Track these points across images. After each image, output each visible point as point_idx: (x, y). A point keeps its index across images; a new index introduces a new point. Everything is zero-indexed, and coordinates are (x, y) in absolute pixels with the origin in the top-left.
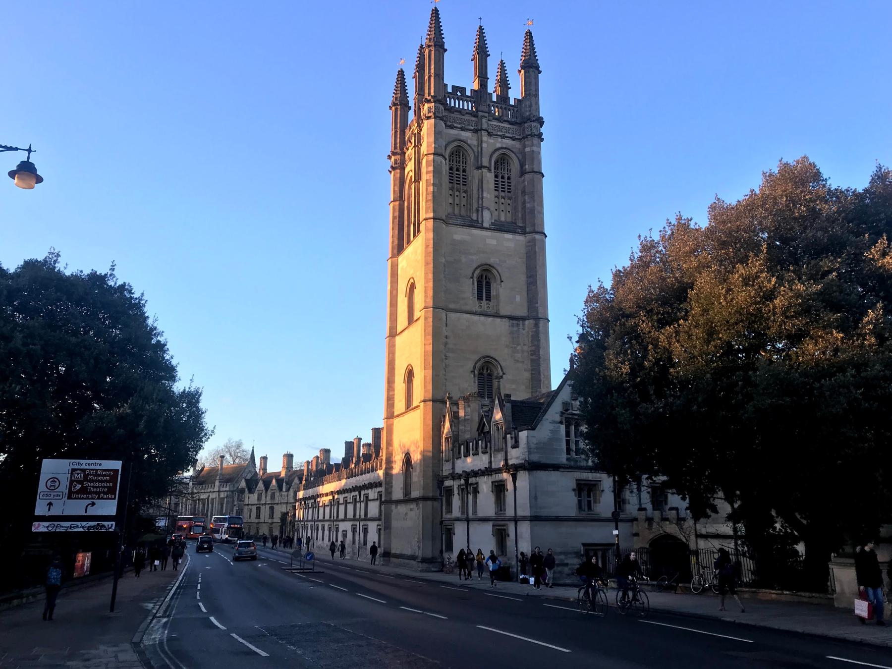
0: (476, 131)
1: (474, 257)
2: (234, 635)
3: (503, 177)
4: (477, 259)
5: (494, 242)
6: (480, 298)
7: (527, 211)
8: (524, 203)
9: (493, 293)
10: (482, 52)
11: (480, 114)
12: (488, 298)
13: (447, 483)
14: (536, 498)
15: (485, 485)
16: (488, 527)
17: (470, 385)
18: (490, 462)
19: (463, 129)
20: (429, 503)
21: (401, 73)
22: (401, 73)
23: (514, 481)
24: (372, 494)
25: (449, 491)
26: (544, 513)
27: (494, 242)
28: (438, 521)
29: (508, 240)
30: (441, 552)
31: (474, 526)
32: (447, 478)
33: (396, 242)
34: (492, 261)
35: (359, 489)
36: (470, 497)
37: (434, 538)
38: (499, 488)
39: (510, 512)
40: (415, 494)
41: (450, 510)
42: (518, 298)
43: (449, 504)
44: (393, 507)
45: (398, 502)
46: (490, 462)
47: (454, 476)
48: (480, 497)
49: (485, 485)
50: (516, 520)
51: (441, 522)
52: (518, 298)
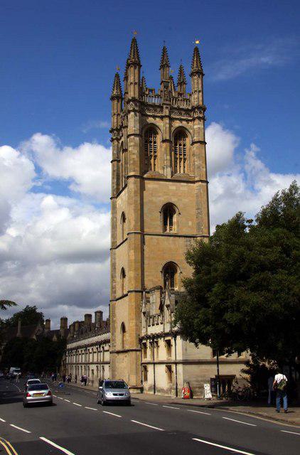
0: (162, 118)
1: (162, 199)
2: (12, 425)
3: (180, 145)
4: (162, 200)
5: (174, 188)
6: (165, 224)
7: (196, 167)
8: (194, 162)
10: (164, 65)
11: (165, 106)
12: (171, 224)
13: (144, 341)
14: (186, 350)
15: (162, 342)
16: (164, 367)
18: (164, 328)
19: (154, 117)
20: (134, 352)
21: (117, 76)
22: (117, 76)
23: (175, 340)
25: (145, 344)
26: (191, 358)
27: (174, 188)
28: (140, 363)
29: (182, 186)
30: (142, 381)
32: (143, 338)
33: (115, 187)
34: (173, 200)
35: (100, 343)
36: (155, 350)
37: (137, 373)
38: (168, 343)
39: (173, 358)
40: (127, 348)
41: (146, 357)
42: (190, 223)
43: (145, 353)
44: (116, 355)
45: (118, 352)
46: (164, 328)
47: (148, 337)
48: (160, 348)
49: (162, 342)
50: (176, 363)
52: (190, 223)
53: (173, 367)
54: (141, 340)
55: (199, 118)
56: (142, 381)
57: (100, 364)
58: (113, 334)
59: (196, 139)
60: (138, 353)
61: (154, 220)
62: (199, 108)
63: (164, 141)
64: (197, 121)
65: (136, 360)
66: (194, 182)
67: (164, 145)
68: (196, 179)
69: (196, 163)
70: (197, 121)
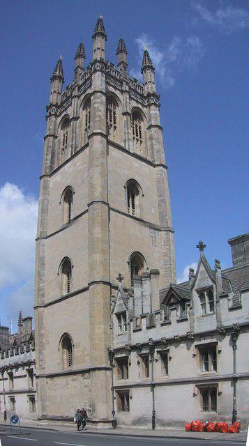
4: (127, 175)
8: (152, 145)
9: (137, 203)
17: (126, 271)
24: (22, 371)
30: (113, 412)
31: (157, 389)
51: (113, 388)
53: (225, 388)
54: (111, 354)
55: (155, 104)
56: (113, 412)
57: (6, 394)
58: (40, 352)
59: (153, 123)
60: (108, 373)
61: (119, 198)
62: (154, 95)
63: (124, 114)
64: (153, 107)
65: (106, 382)
66: (154, 166)
67: (125, 118)
68: (156, 163)
69: (155, 147)
70: (153, 107)
